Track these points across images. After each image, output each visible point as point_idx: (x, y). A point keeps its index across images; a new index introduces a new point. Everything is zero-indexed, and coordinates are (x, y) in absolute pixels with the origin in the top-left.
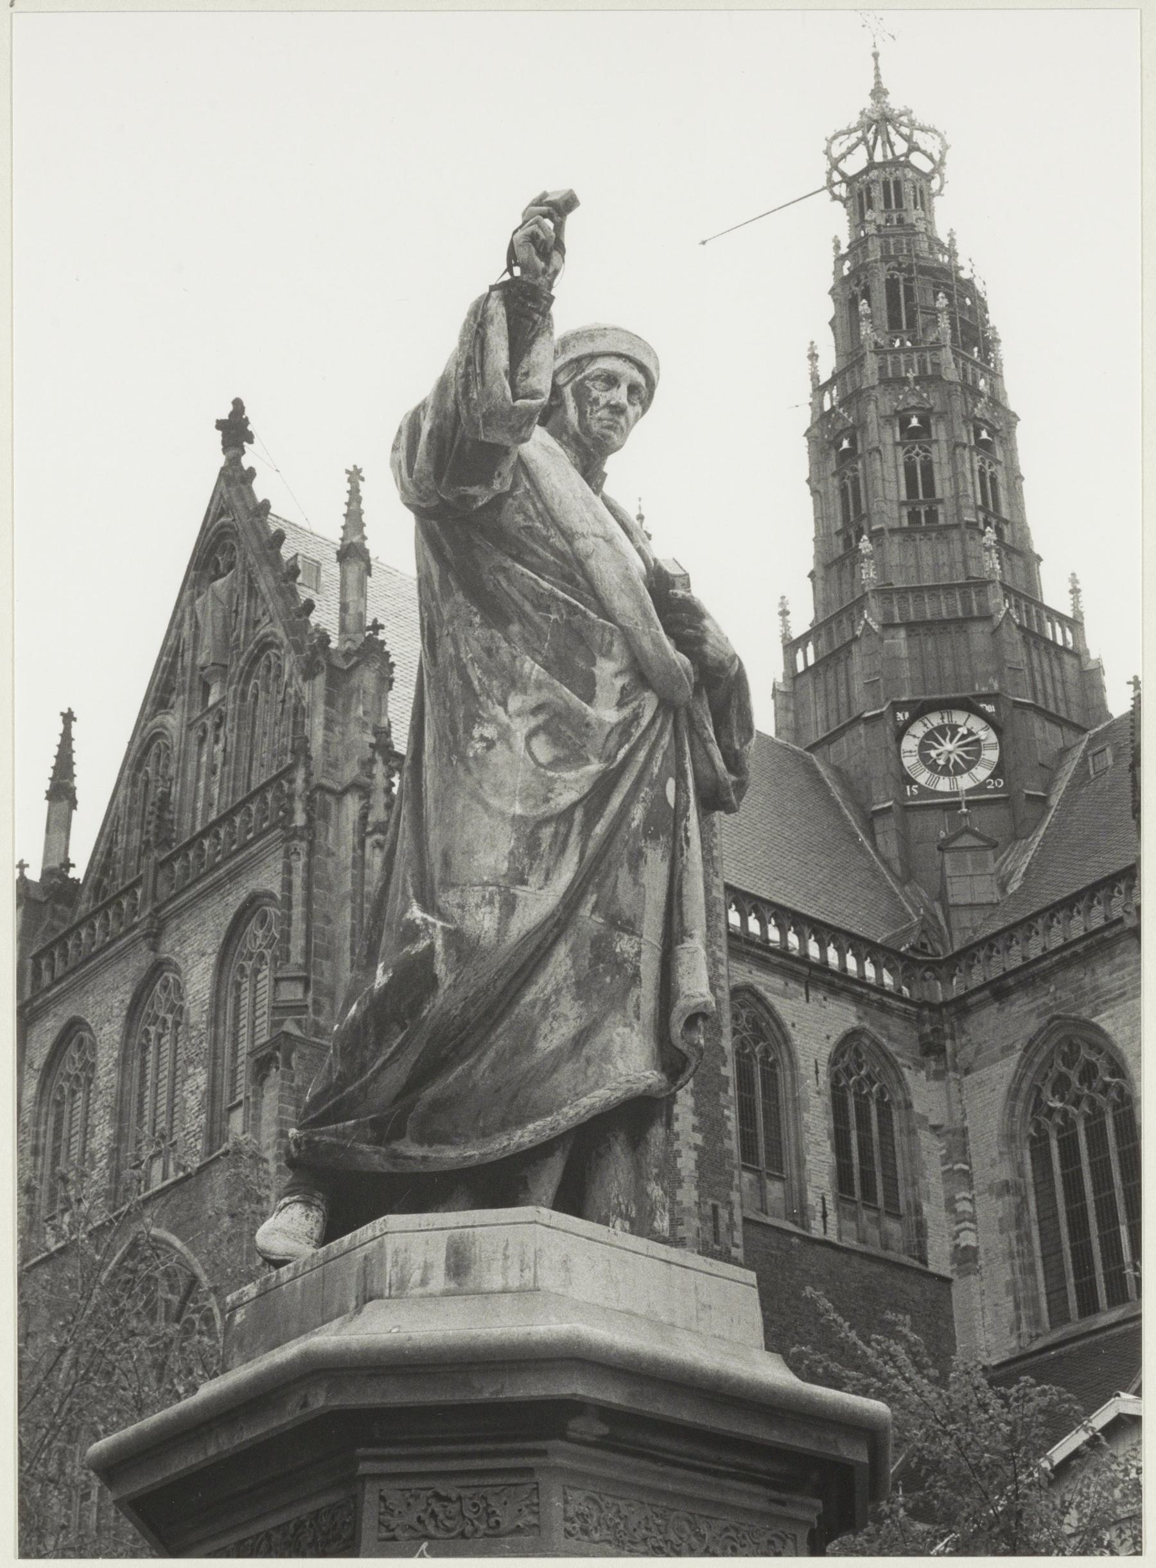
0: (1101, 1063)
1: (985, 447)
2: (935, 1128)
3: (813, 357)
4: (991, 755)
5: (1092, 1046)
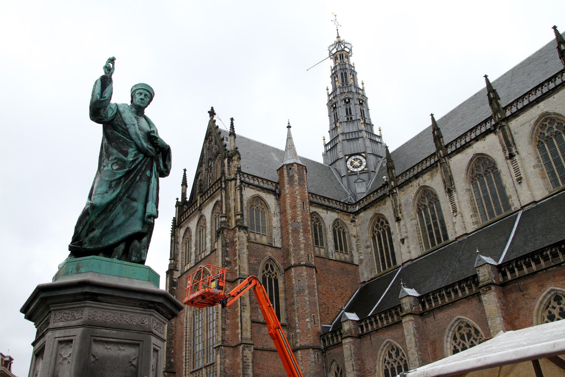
0: (384, 222)
1: (361, 104)
2: (354, 236)
3: (327, 89)
4: (364, 164)
5: (382, 218)
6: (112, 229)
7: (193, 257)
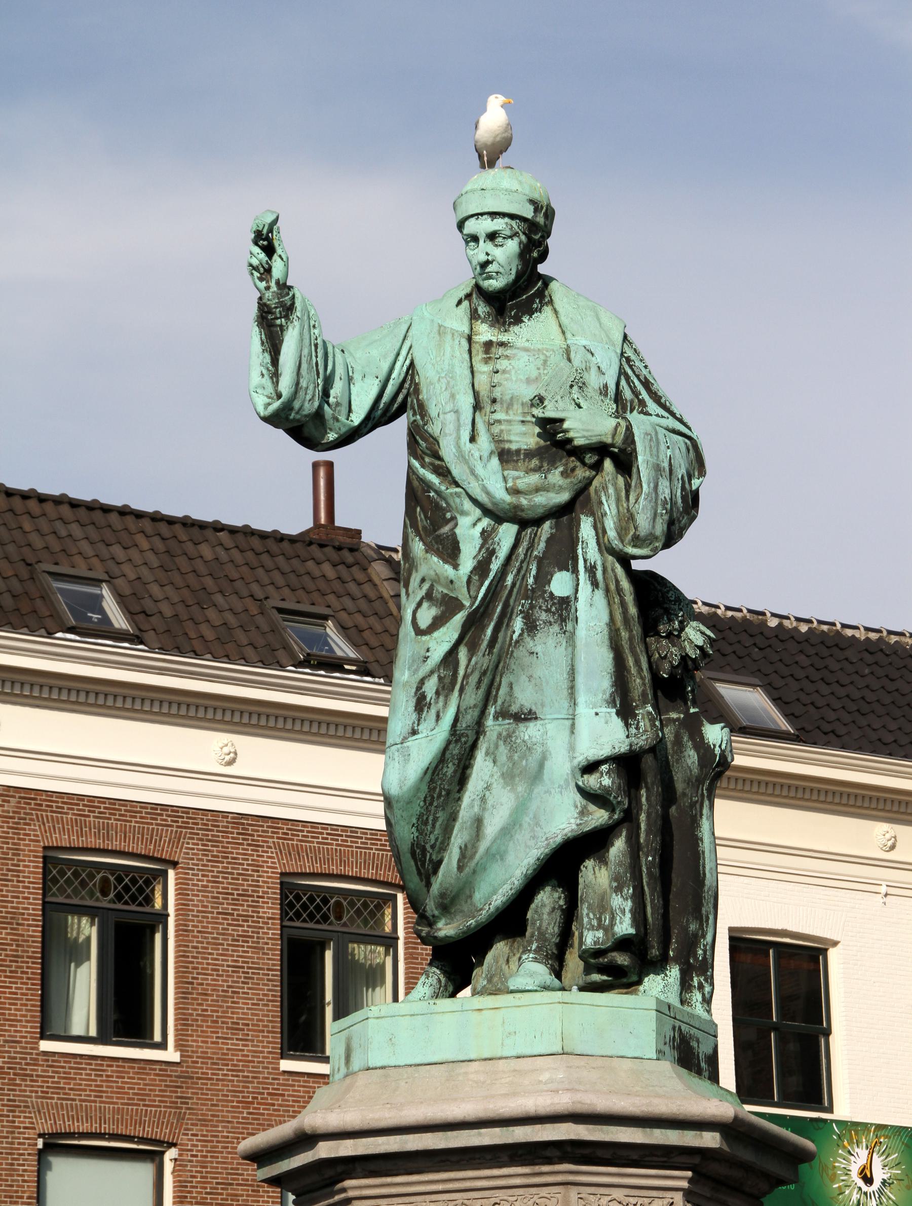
6: (488, 850)
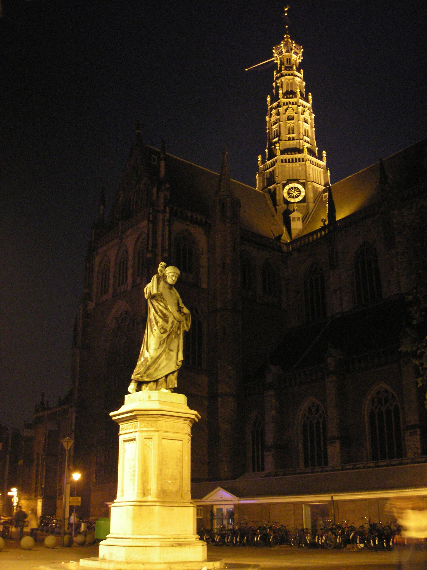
7: (111, 290)
